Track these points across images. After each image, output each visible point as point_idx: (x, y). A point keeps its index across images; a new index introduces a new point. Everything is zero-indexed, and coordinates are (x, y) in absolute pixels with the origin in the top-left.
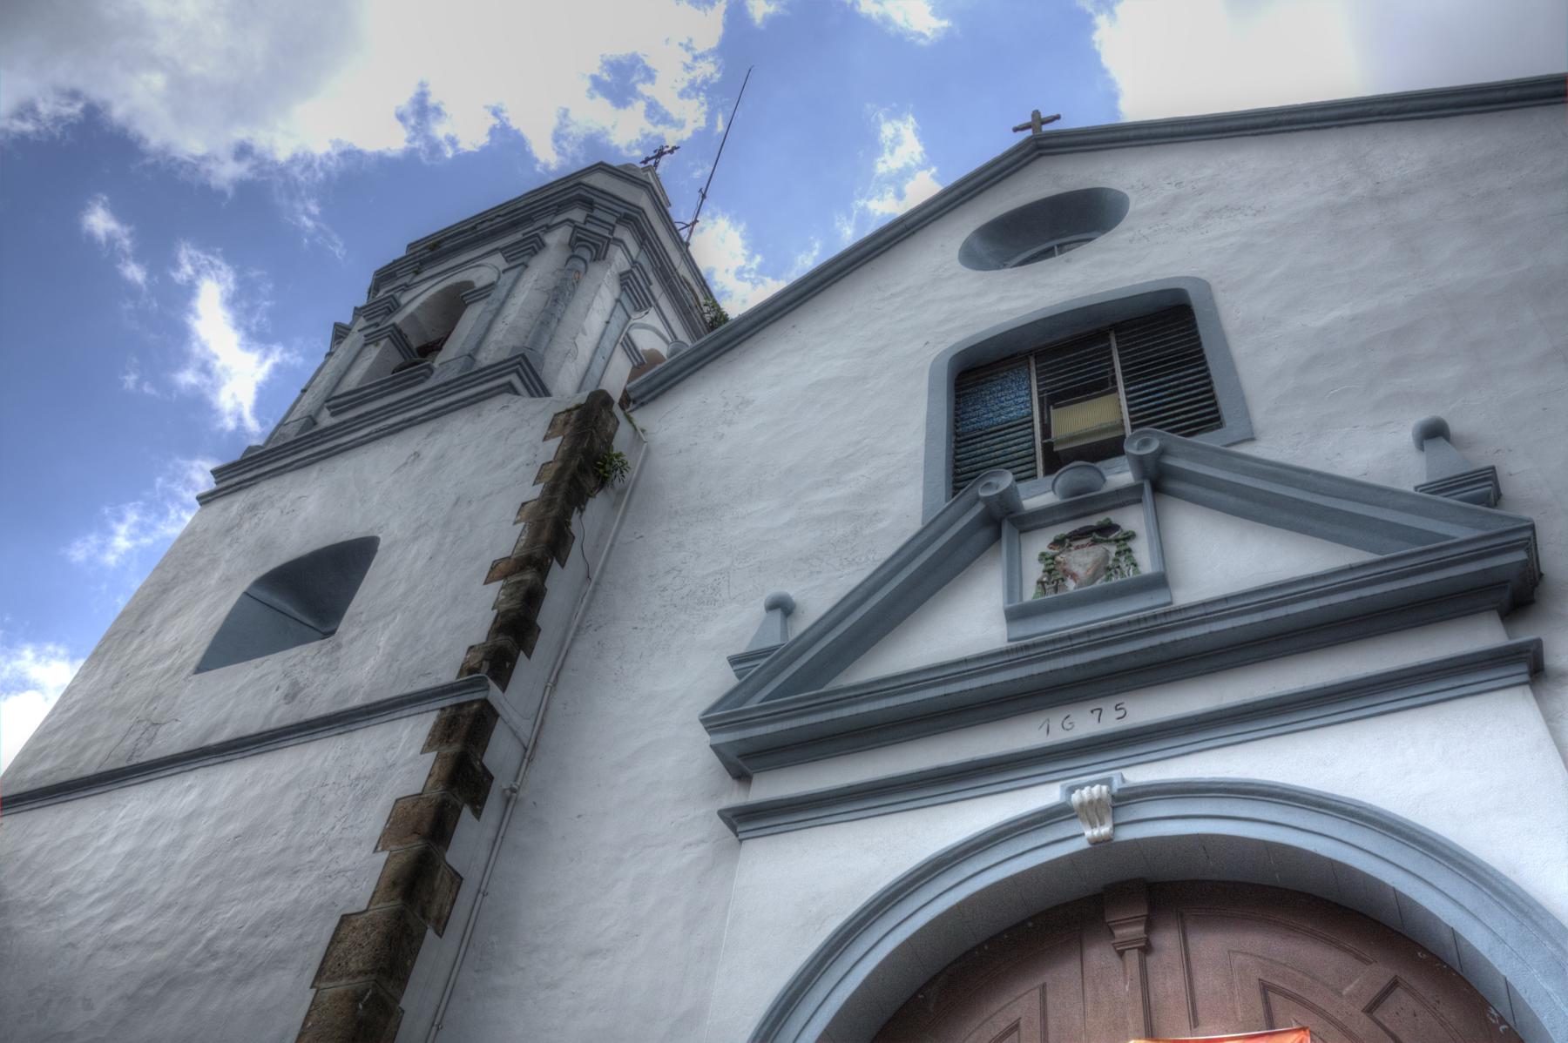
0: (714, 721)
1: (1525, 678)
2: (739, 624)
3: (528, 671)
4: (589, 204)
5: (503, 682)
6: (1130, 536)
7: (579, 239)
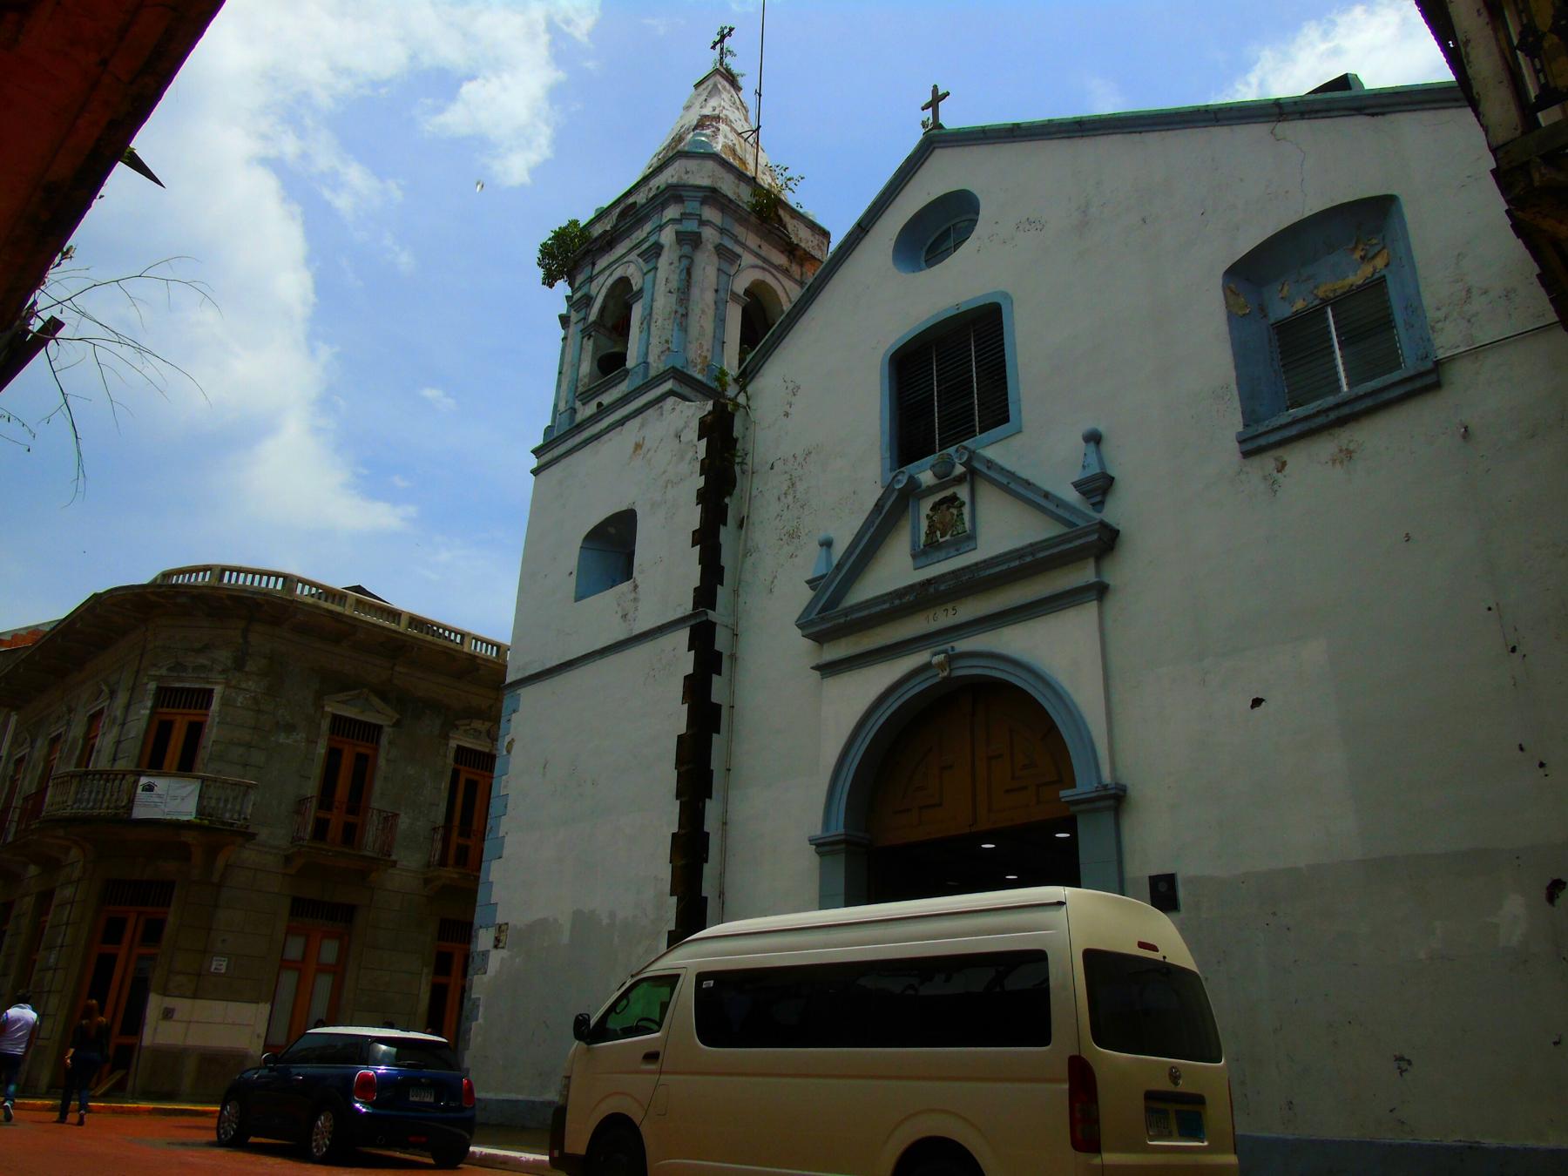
0: (803, 624)
3: (722, 593)
4: (679, 199)
6: (963, 504)
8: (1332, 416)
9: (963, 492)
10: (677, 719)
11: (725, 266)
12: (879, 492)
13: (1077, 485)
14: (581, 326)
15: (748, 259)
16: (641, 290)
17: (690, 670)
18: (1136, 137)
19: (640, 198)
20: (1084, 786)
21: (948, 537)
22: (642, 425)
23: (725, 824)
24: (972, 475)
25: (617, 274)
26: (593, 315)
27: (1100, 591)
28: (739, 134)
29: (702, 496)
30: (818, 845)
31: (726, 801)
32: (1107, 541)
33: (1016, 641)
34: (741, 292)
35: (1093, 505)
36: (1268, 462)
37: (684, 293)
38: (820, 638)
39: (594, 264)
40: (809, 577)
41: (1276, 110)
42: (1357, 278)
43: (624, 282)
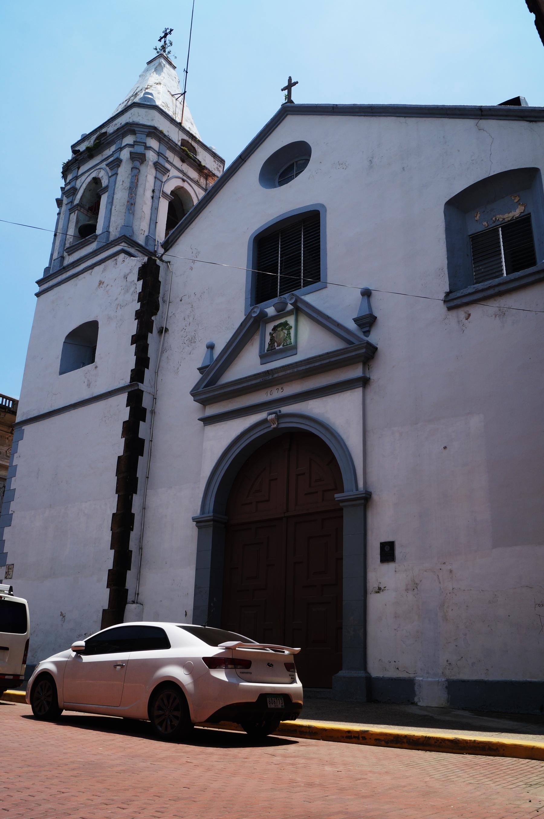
0: (195, 393)
1: (361, 385)
2: (198, 357)
3: (148, 373)
4: (133, 132)
5: (142, 382)
6: (291, 327)
7: (134, 158)
8: (497, 290)
9: (291, 320)
10: (118, 447)
11: (159, 176)
12: (243, 318)
13: (355, 320)
14: (69, 206)
15: (173, 172)
16: (107, 187)
17: (127, 418)
18: (402, 119)
19: (110, 129)
20: (348, 492)
21: (281, 347)
22: (104, 270)
23: (144, 508)
24: (297, 311)
25: (94, 175)
26: (77, 201)
27: (364, 382)
28: (173, 95)
29: (138, 315)
30: (197, 522)
31: (145, 496)
32: (369, 355)
33: (315, 408)
34: (169, 192)
35: (364, 332)
36: (461, 313)
37: (133, 188)
38: (205, 403)
39: (79, 168)
40: (200, 366)
41: (480, 113)
42: (517, 213)
43: (96, 181)
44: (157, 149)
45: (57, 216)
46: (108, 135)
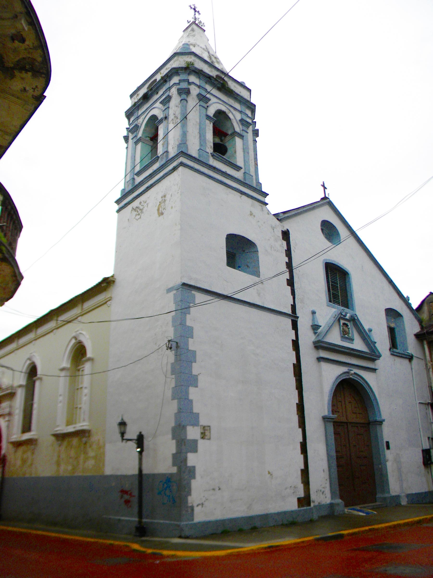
7: (181, 93)
14: (135, 140)
15: (213, 100)
34: (212, 116)
44: (198, 84)
45: (126, 150)
46: (158, 80)
